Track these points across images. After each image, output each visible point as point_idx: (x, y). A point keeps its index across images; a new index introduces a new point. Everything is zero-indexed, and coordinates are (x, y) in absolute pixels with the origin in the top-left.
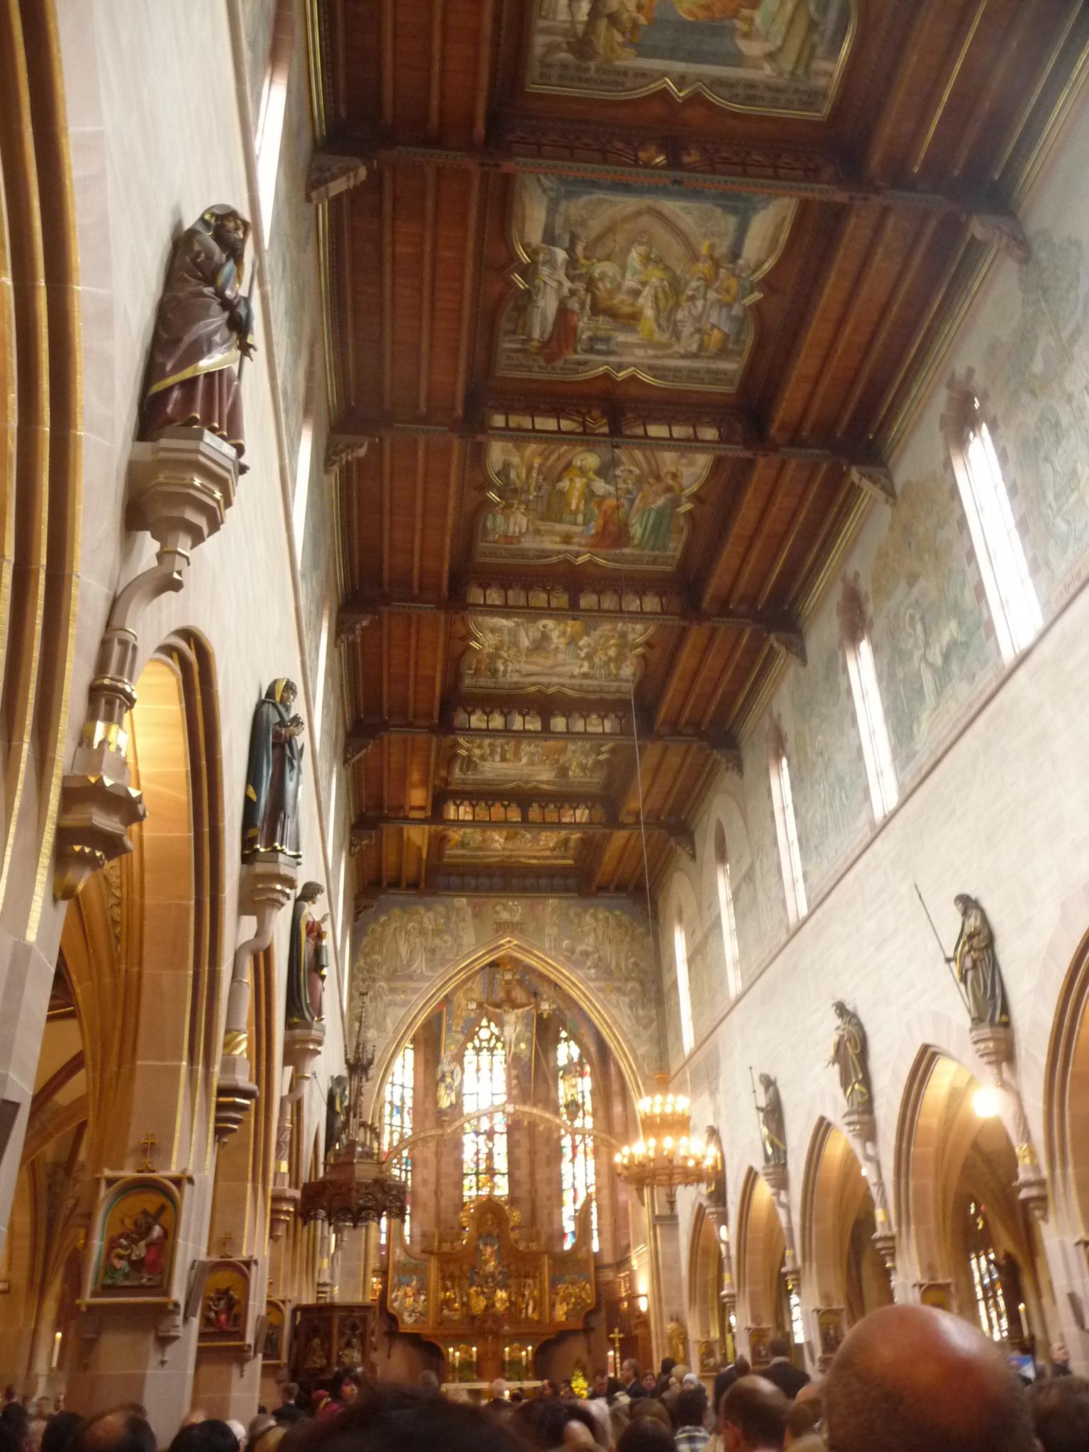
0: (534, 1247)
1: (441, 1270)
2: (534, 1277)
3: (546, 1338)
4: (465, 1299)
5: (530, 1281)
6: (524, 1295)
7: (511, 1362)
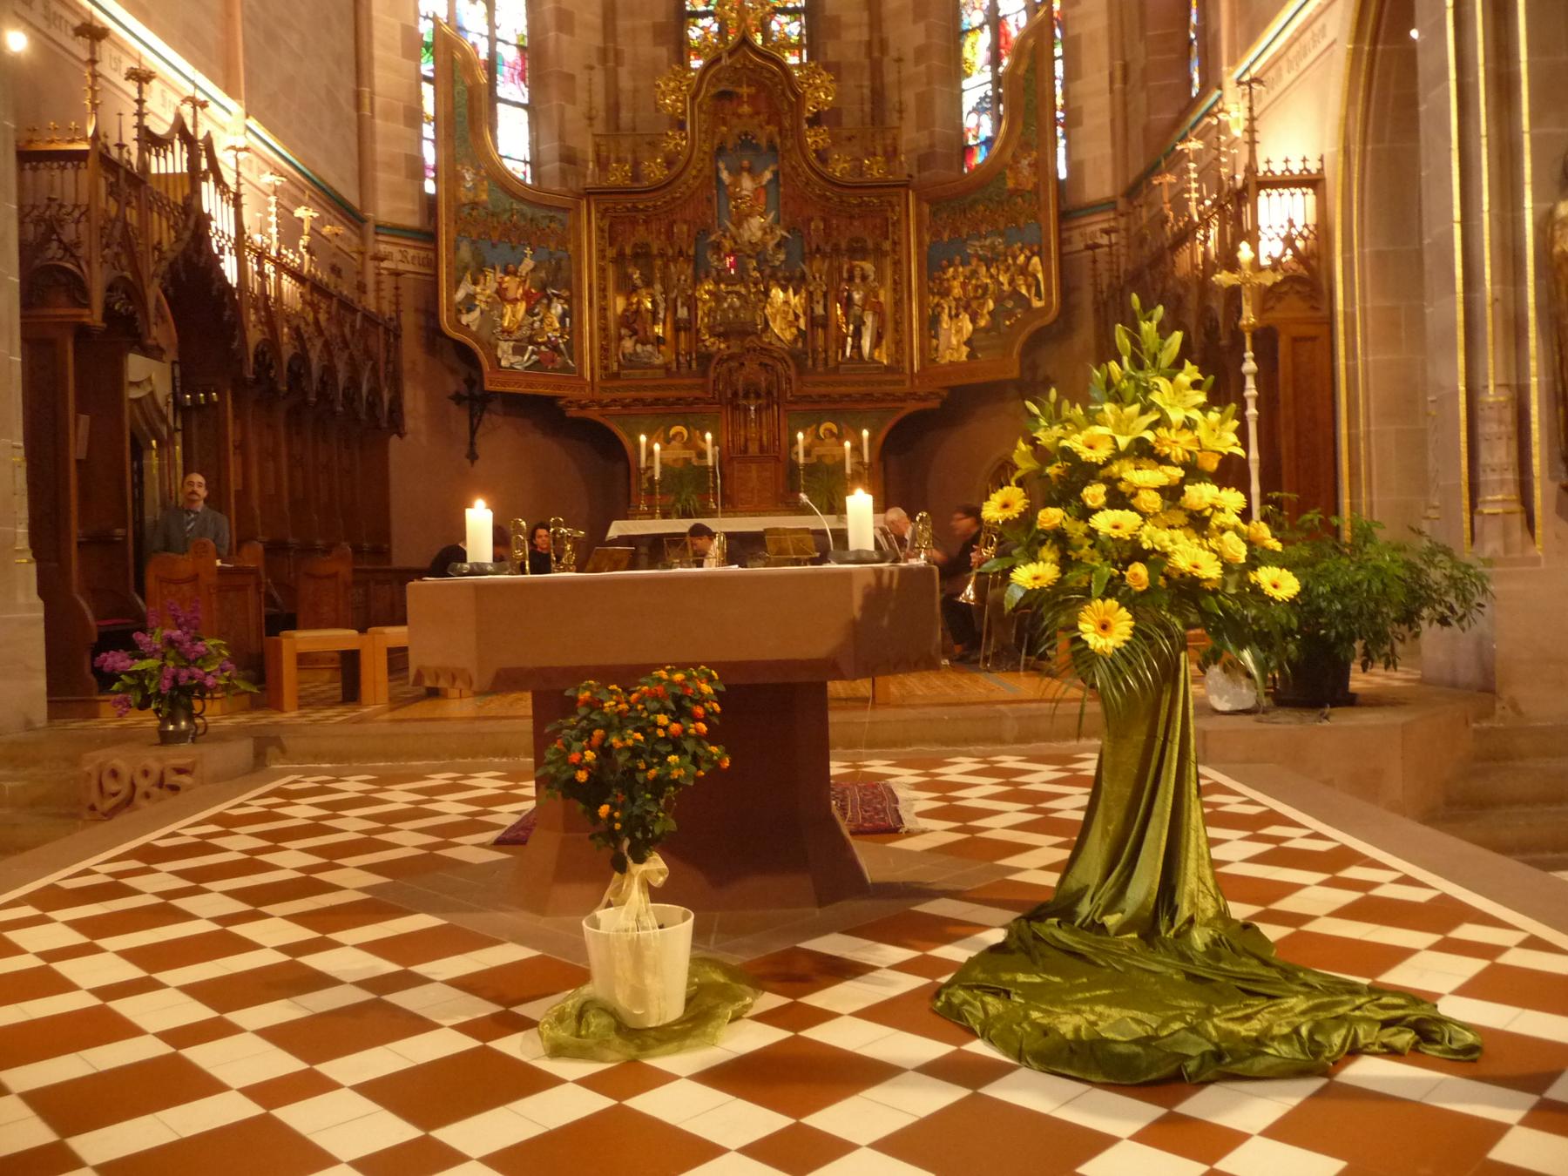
0: (876, 170)
1: (611, 236)
2: (878, 254)
3: (911, 407)
4: (683, 313)
5: (869, 267)
6: (848, 304)
7: (811, 469)
